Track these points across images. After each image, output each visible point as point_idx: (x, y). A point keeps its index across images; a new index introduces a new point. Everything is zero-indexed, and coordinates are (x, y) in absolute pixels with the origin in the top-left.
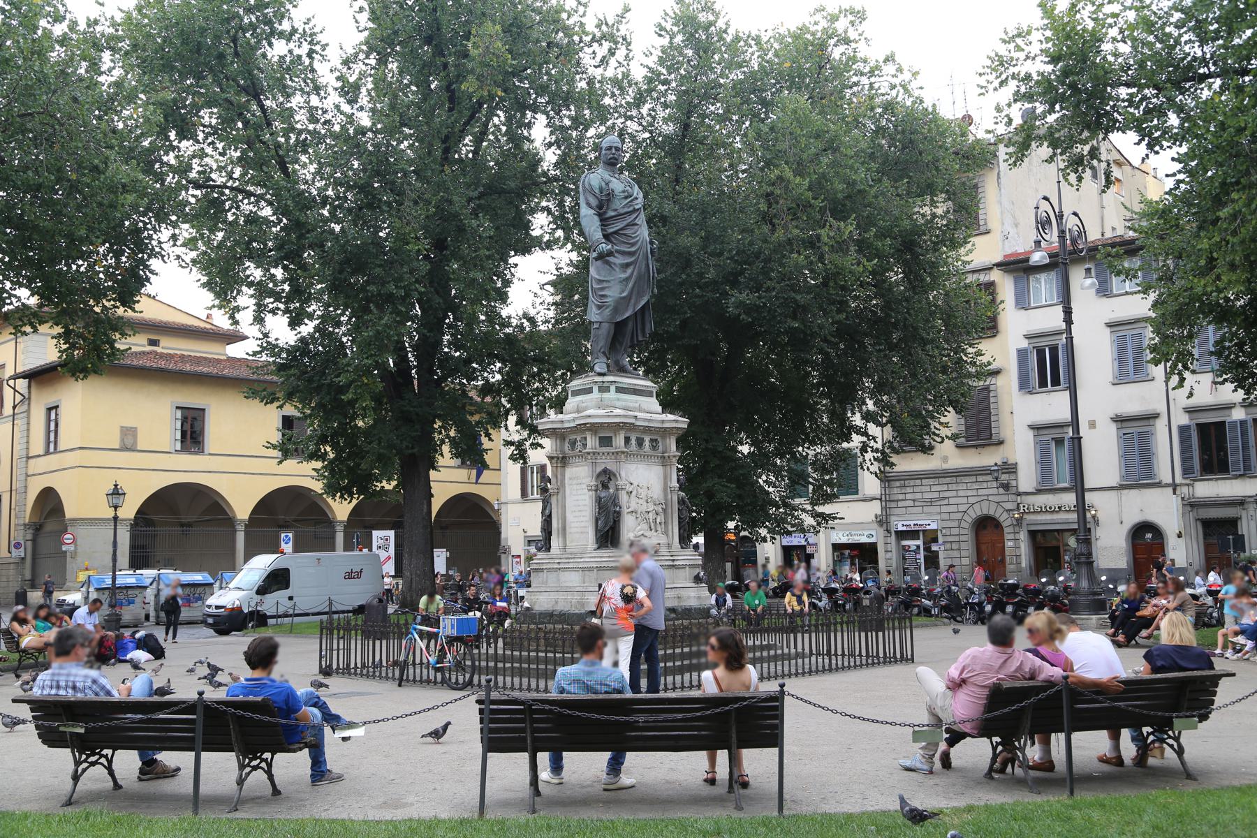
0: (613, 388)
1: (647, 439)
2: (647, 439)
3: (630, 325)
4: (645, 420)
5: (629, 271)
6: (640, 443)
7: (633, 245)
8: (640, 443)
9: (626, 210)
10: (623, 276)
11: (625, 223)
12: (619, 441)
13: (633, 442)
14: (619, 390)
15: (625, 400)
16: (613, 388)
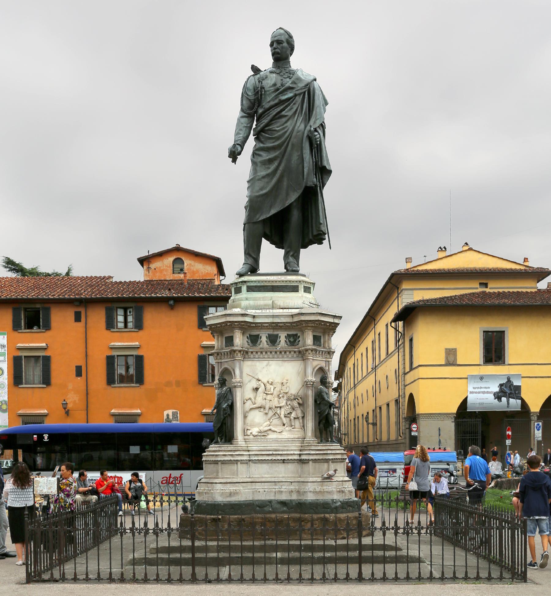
0: (244, 288)
1: (283, 336)
2: (283, 336)
3: (296, 215)
4: (267, 317)
5: (273, 167)
6: (273, 340)
7: (278, 138)
8: (273, 340)
9: (272, 103)
10: (264, 173)
11: (269, 118)
12: (239, 340)
13: (264, 339)
14: (250, 289)
15: (255, 299)
16: (244, 288)
